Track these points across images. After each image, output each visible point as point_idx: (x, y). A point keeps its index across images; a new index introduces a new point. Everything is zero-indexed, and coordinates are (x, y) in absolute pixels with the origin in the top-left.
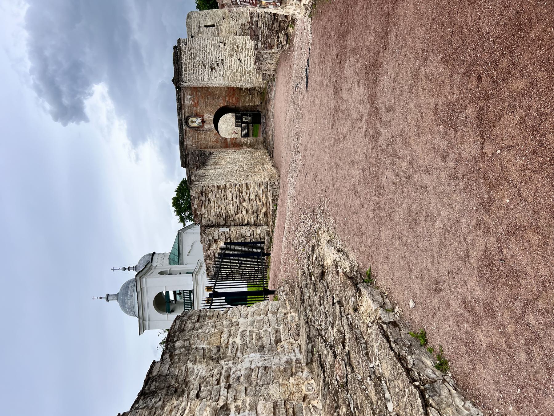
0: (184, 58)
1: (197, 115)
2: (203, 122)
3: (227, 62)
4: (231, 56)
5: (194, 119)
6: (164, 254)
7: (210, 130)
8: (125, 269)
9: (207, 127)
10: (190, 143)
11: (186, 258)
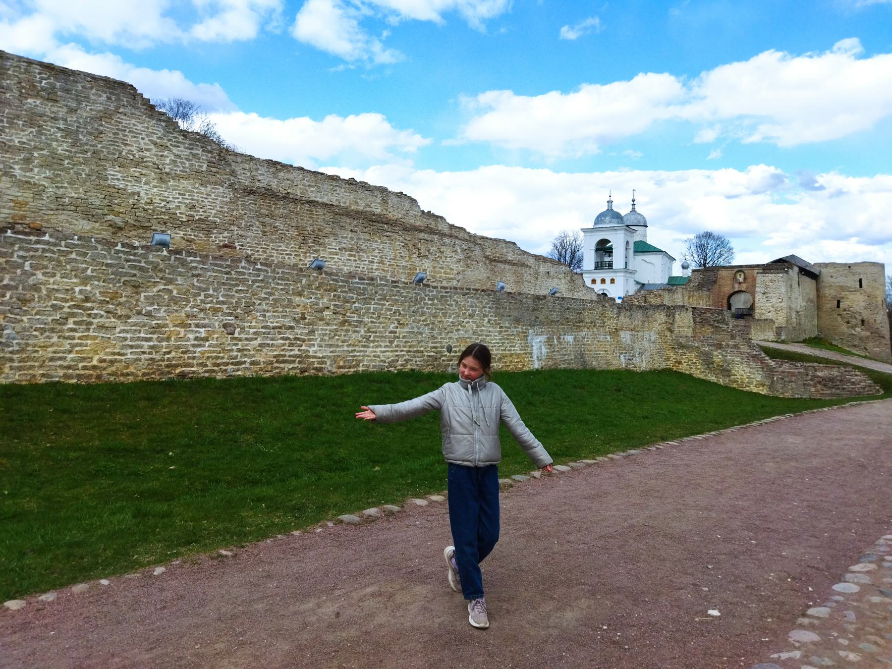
0: (772, 275)
1: (745, 279)
2: (740, 283)
3: (768, 304)
4: (773, 306)
5: (742, 276)
6: (645, 236)
7: (733, 287)
8: (633, 201)
9: (736, 285)
10: (723, 273)
11: (640, 258)
